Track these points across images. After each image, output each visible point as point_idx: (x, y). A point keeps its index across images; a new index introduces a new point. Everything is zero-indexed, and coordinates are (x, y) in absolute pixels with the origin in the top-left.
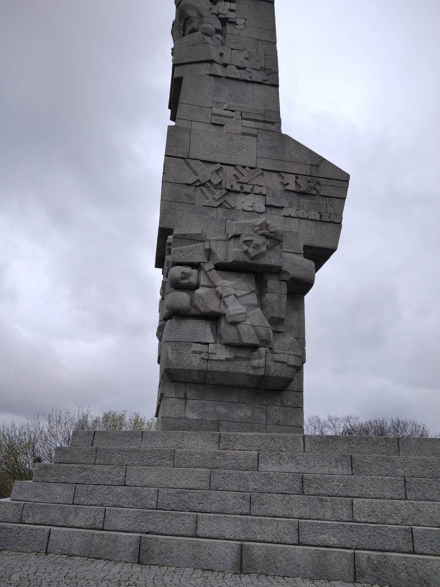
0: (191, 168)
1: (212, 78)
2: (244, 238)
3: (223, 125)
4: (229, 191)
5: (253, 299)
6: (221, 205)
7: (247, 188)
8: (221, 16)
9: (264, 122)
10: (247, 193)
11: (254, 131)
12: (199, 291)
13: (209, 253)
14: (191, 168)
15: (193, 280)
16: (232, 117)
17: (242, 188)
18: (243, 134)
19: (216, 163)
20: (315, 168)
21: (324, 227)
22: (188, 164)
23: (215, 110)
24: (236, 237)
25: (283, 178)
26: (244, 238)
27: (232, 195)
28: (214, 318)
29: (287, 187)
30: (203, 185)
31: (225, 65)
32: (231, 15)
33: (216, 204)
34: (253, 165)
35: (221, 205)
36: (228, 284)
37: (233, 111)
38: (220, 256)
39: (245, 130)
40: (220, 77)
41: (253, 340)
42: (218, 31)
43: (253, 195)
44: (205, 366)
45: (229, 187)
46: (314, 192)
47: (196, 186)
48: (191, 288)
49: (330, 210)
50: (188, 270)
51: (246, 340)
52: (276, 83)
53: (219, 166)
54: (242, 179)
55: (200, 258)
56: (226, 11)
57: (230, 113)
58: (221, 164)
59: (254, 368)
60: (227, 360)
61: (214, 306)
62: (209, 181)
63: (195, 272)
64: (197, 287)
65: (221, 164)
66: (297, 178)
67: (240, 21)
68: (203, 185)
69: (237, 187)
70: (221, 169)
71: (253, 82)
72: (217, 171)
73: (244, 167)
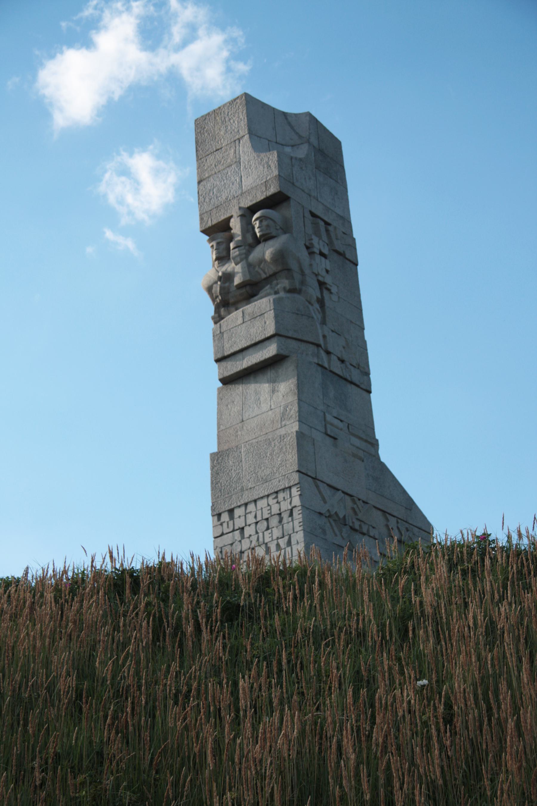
0: (320, 492)
1: (319, 369)
3: (335, 439)
8: (320, 278)
9: (366, 441)
10: (364, 534)
11: (361, 454)
14: (320, 492)
16: (341, 429)
17: (360, 526)
18: (354, 455)
19: (338, 490)
22: (317, 487)
25: (387, 520)
31: (328, 353)
34: (365, 499)
37: (341, 421)
40: (326, 368)
43: (368, 538)
45: (351, 524)
47: (326, 517)
52: (368, 389)
54: (360, 516)
56: (324, 273)
58: (343, 492)
65: (343, 492)
66: (398, 522)
67: (334, 289)
69: (357, 527)
71: (352, 383)
73: (359, 500)
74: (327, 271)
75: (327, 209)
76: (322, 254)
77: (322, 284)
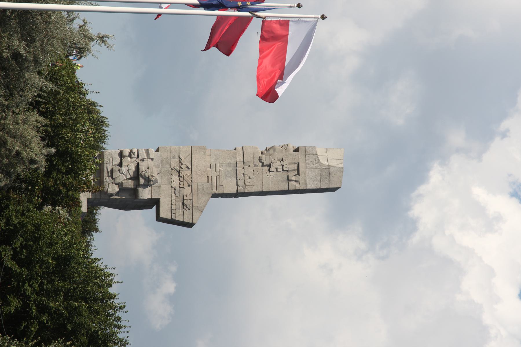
2: (147, 170)
4: (179, 172)
5: (129, 177)
6: (172, 169)
7: (181, 179)
11: (210, 181)
12: (129, 158)
13: (143, 160)
15: (133, 156)
20: (197, 208)
21: (169, 211)
23: (218, 165)
24: (148, 168)
26: (147, 170)
27: (177, 174)
28: (120, 165)
29: (185, 196)
30: (180, 162)
32: (273, 169)
33: (172, 168)
35: (172, 169)
36: (133, 168)
38: (141, 164)
39: (210, 178)
41: (114, 177)
42: (263, 163)
44: (105, 163)
46: (185, 207)
48: (130, 156)
49: (177, 215)
50: (136, 154)
51: (114, 174)
53: (190, 167)
55: (140, 157)
57: (218, 170)
59: (106, 179)
60: (108, 169)
61: (124, 164)
62: (182, 164)
63: (136, 156)
64: (131, 158)
68: (180, 162)
69: (181, 175)
70: (189, 168)
72: (187, 167)
74: (277, 169)
75: (305, 174)
76: (283, 166)
77: (269, 166)
